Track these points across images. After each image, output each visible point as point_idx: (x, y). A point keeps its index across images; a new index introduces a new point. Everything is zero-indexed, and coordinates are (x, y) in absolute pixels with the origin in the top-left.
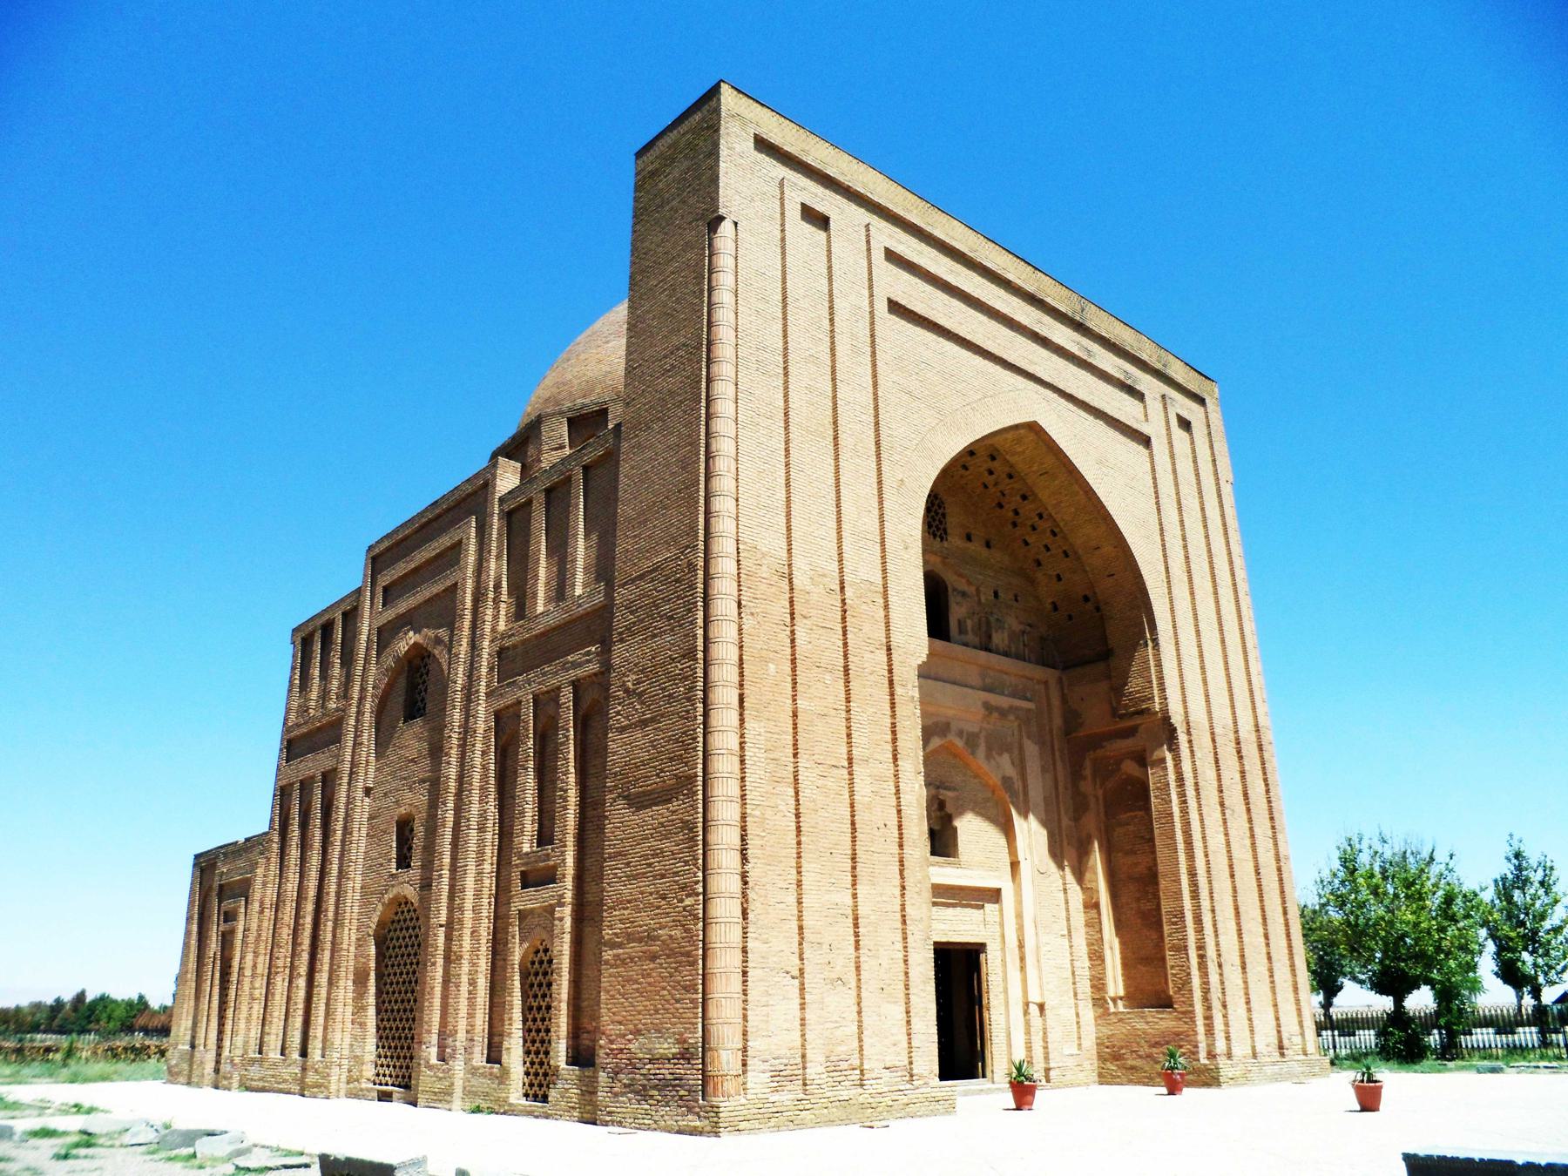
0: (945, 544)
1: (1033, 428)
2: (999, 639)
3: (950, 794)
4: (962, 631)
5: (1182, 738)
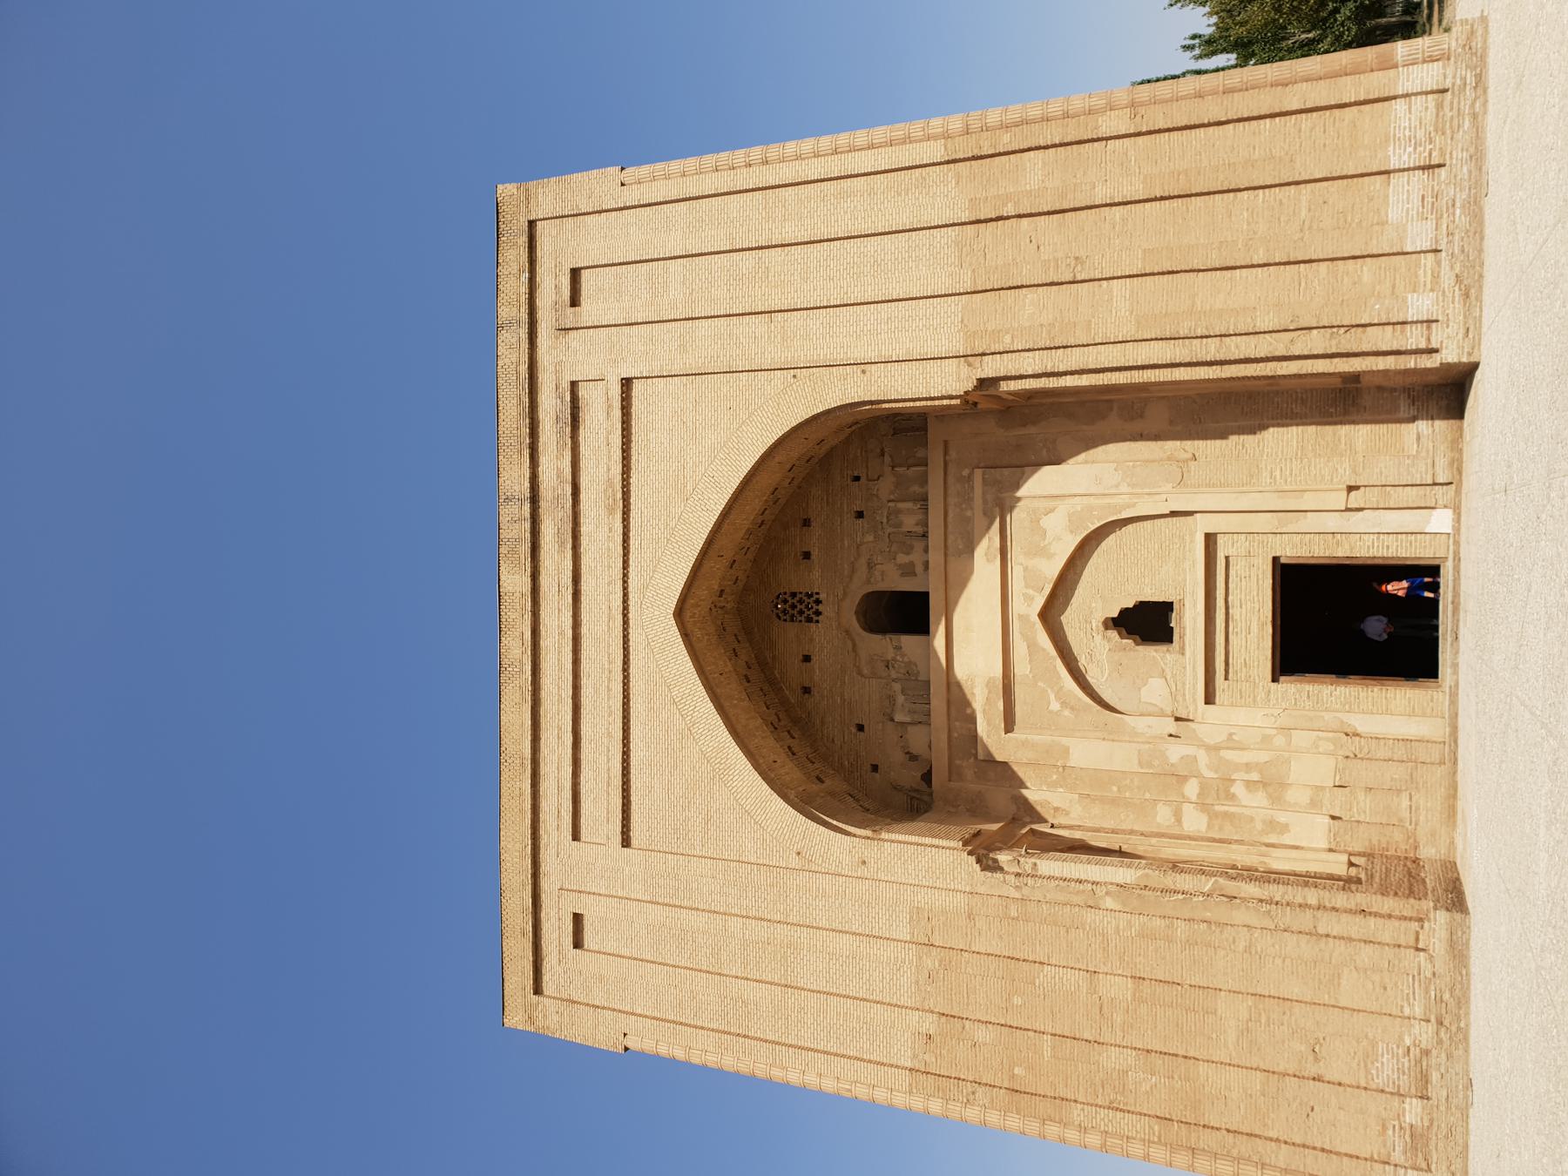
0: (822, 597)
1: (679, 614)
2: (910, 523)
4: (908, 571)
5: (990, 368)
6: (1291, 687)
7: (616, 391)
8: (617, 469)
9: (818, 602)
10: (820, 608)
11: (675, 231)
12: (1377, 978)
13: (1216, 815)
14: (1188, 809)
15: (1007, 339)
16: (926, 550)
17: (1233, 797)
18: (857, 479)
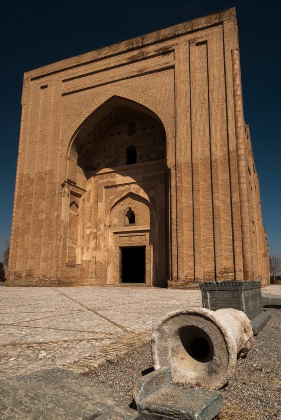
0: (135, 135)
1: (115, 97)
4: (141, 157)
5: (173, 172)
6: (118, 251)
7: (171, 64)
8: (150, 70)
9: (133, 134)
10: (131, 135)
11: (216, 72)
12: (46, 270)
13: (89, 236)
14: (90, 230)
15: (179, 175)
16: (147, 161)
17: (94, 239)
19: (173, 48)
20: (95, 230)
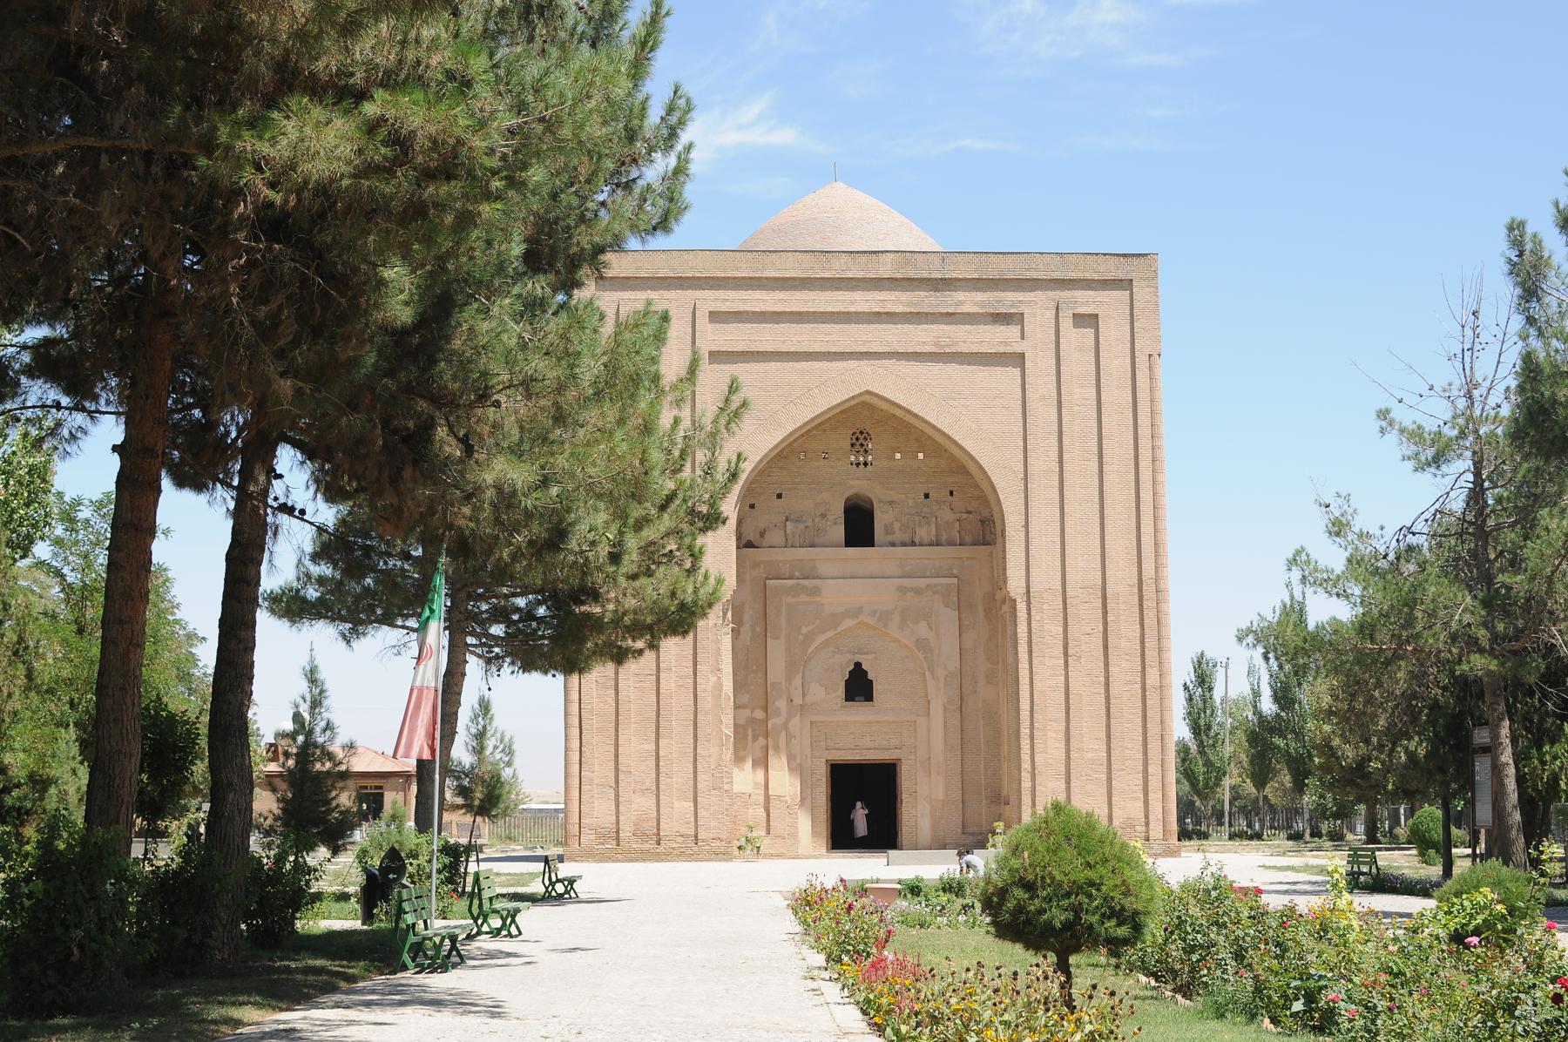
1: (868, 392)
3: (870, 657)
4: (888, 530)
5: (1021, 607)
6: (822, 774)
7: (1018, 349)
16: (904, 545)
17: (755, 738)
18: (951, 493)
19: (1020, 310)
20: (759, 714)
